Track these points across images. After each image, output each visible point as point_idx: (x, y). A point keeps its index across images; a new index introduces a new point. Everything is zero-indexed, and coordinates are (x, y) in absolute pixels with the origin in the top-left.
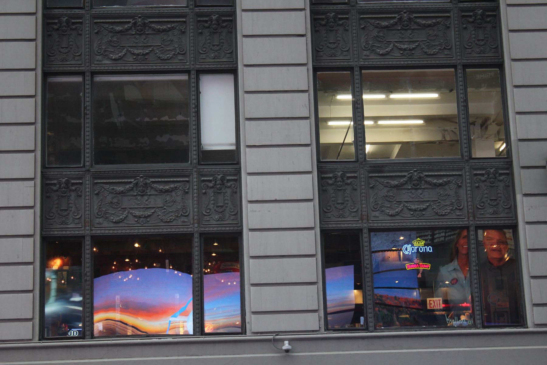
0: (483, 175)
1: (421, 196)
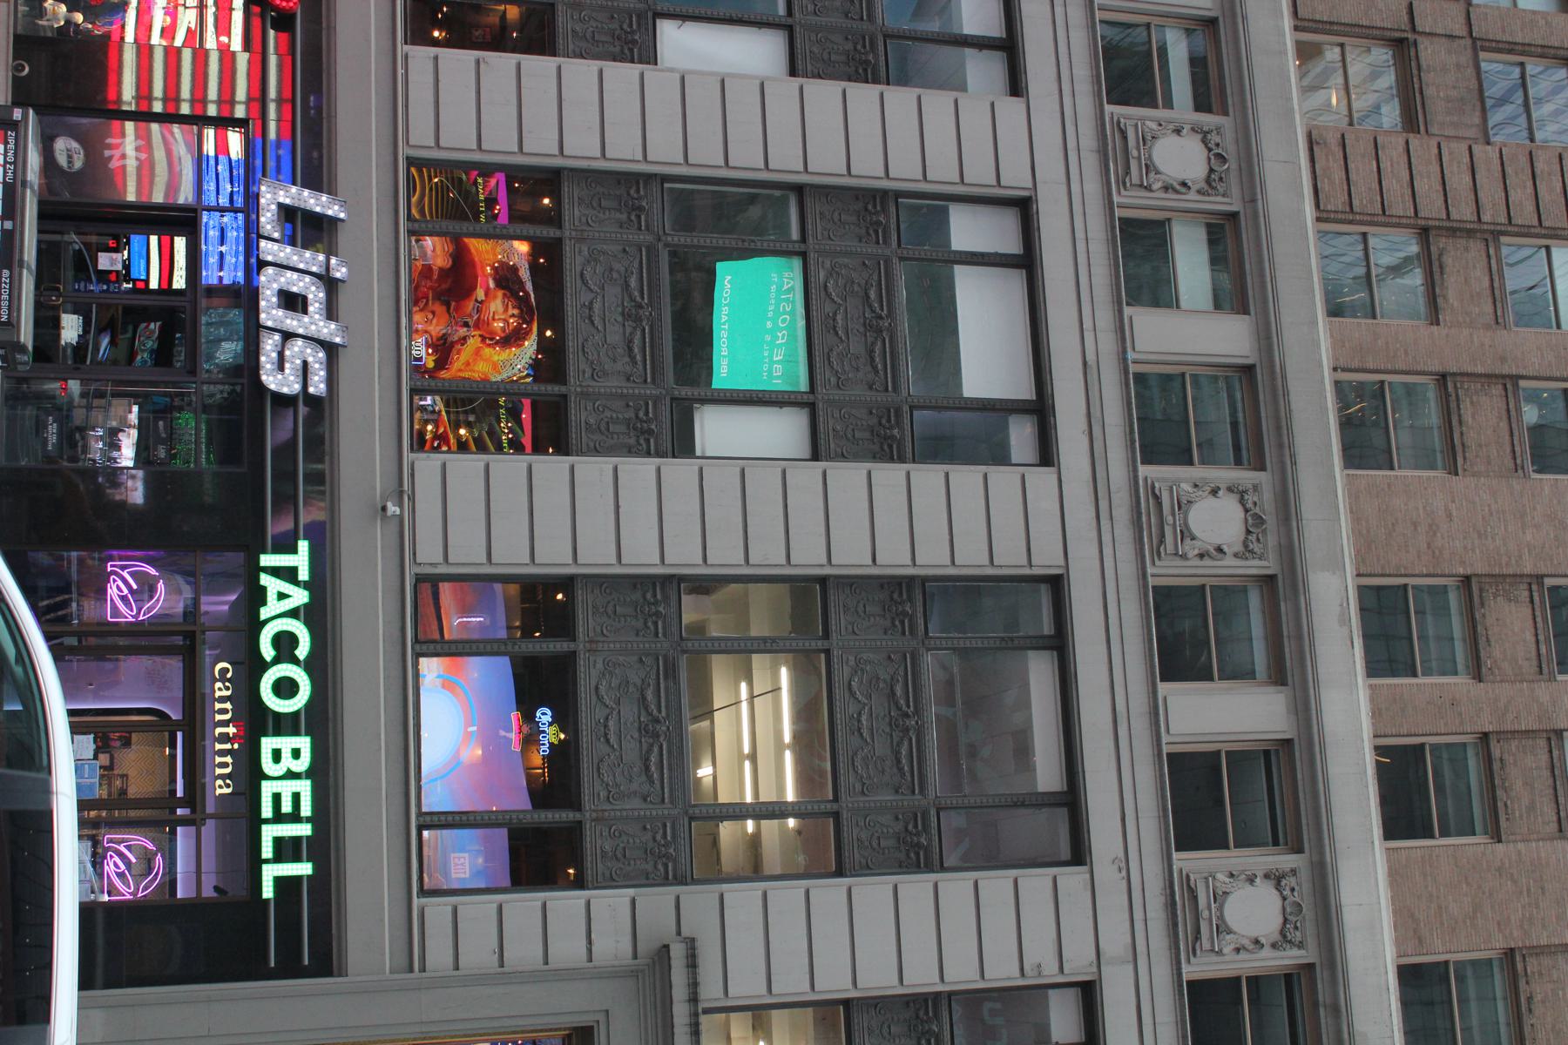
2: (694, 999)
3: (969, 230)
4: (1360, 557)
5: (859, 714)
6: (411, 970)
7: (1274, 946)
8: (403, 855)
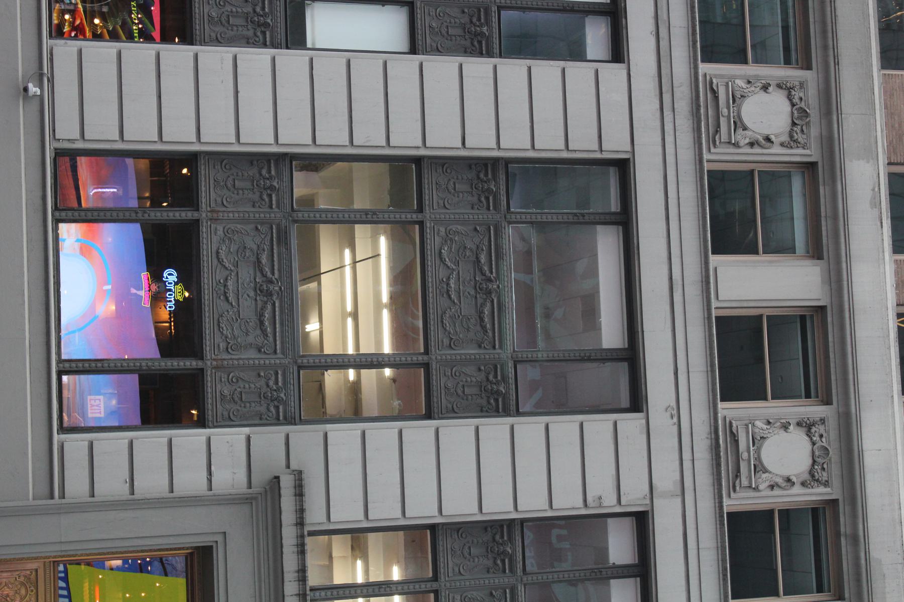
0: (276, 383)
1: (245, 295)
2: (300, 523)
4: (892, 148)
6: (52, 497)
7: (803, 484)
8: (44, 397)
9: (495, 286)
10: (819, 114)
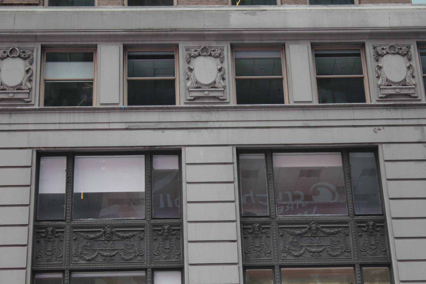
3: (54, 184)
5: (311, 252)
7: (410, 60)
9: (108, 229)
10: (205, 41)
